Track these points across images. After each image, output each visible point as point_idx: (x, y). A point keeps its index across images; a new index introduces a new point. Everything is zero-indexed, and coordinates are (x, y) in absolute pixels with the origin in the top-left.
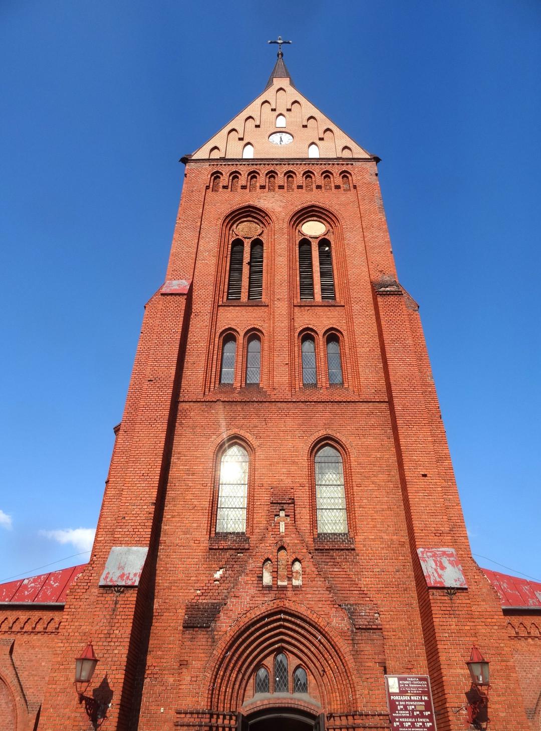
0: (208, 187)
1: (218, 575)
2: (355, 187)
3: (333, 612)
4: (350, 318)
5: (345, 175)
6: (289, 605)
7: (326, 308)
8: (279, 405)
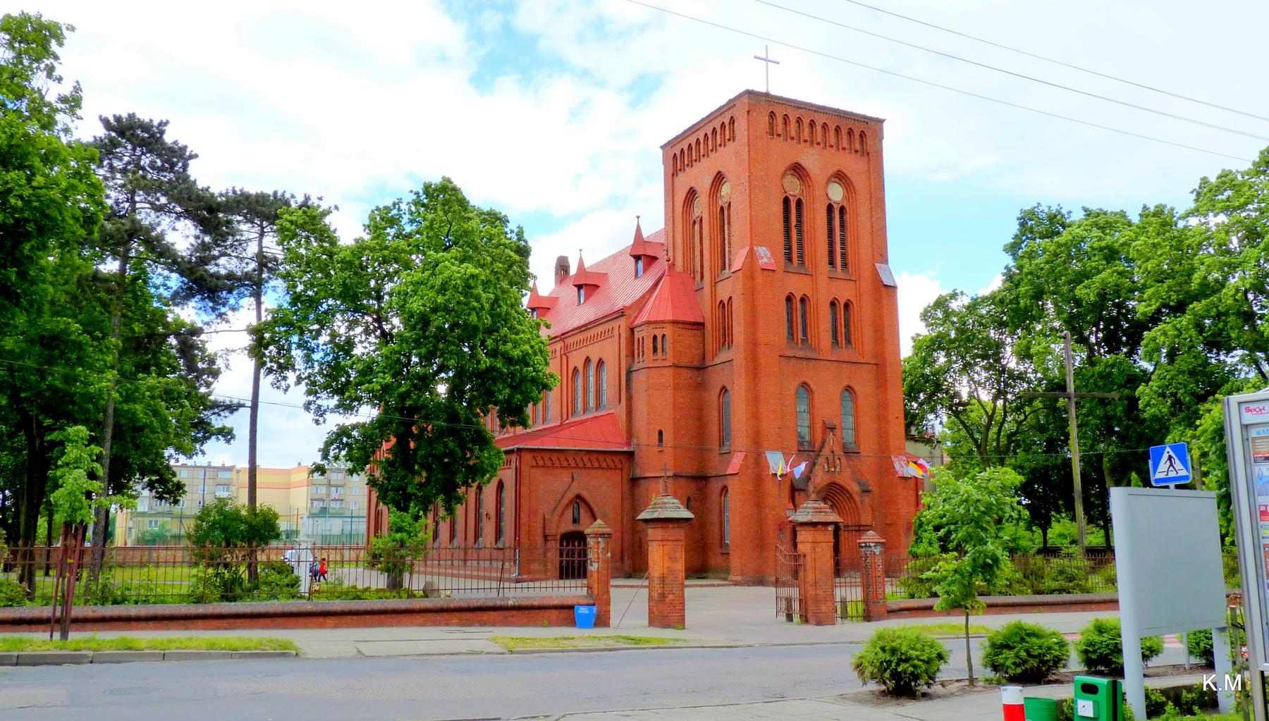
2: (868, 154)
3: (853, 484)
4: (859, 296)
5: (862, 135)
8: (825, 362)
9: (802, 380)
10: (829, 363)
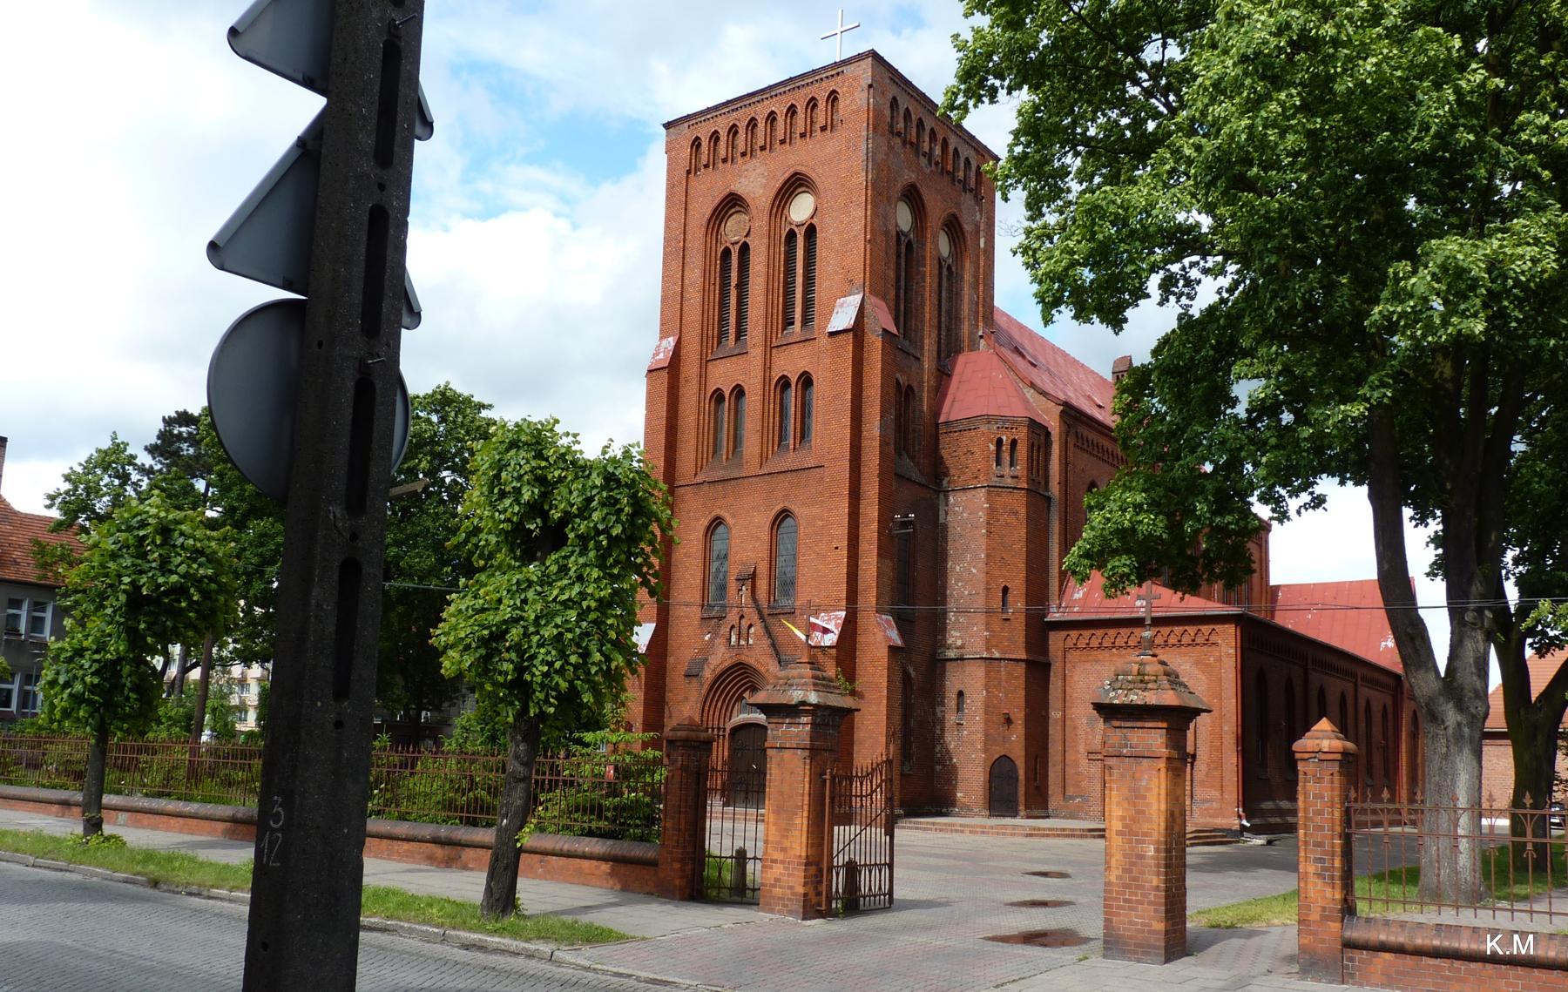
0: (689, 172)
1: (707, 638)
3: (771, 662)
5: (833, 97)
6: (744, 659)
7: (801, 345)
8: (750, 479)
9: (714, 514)
10: (757, 479)
